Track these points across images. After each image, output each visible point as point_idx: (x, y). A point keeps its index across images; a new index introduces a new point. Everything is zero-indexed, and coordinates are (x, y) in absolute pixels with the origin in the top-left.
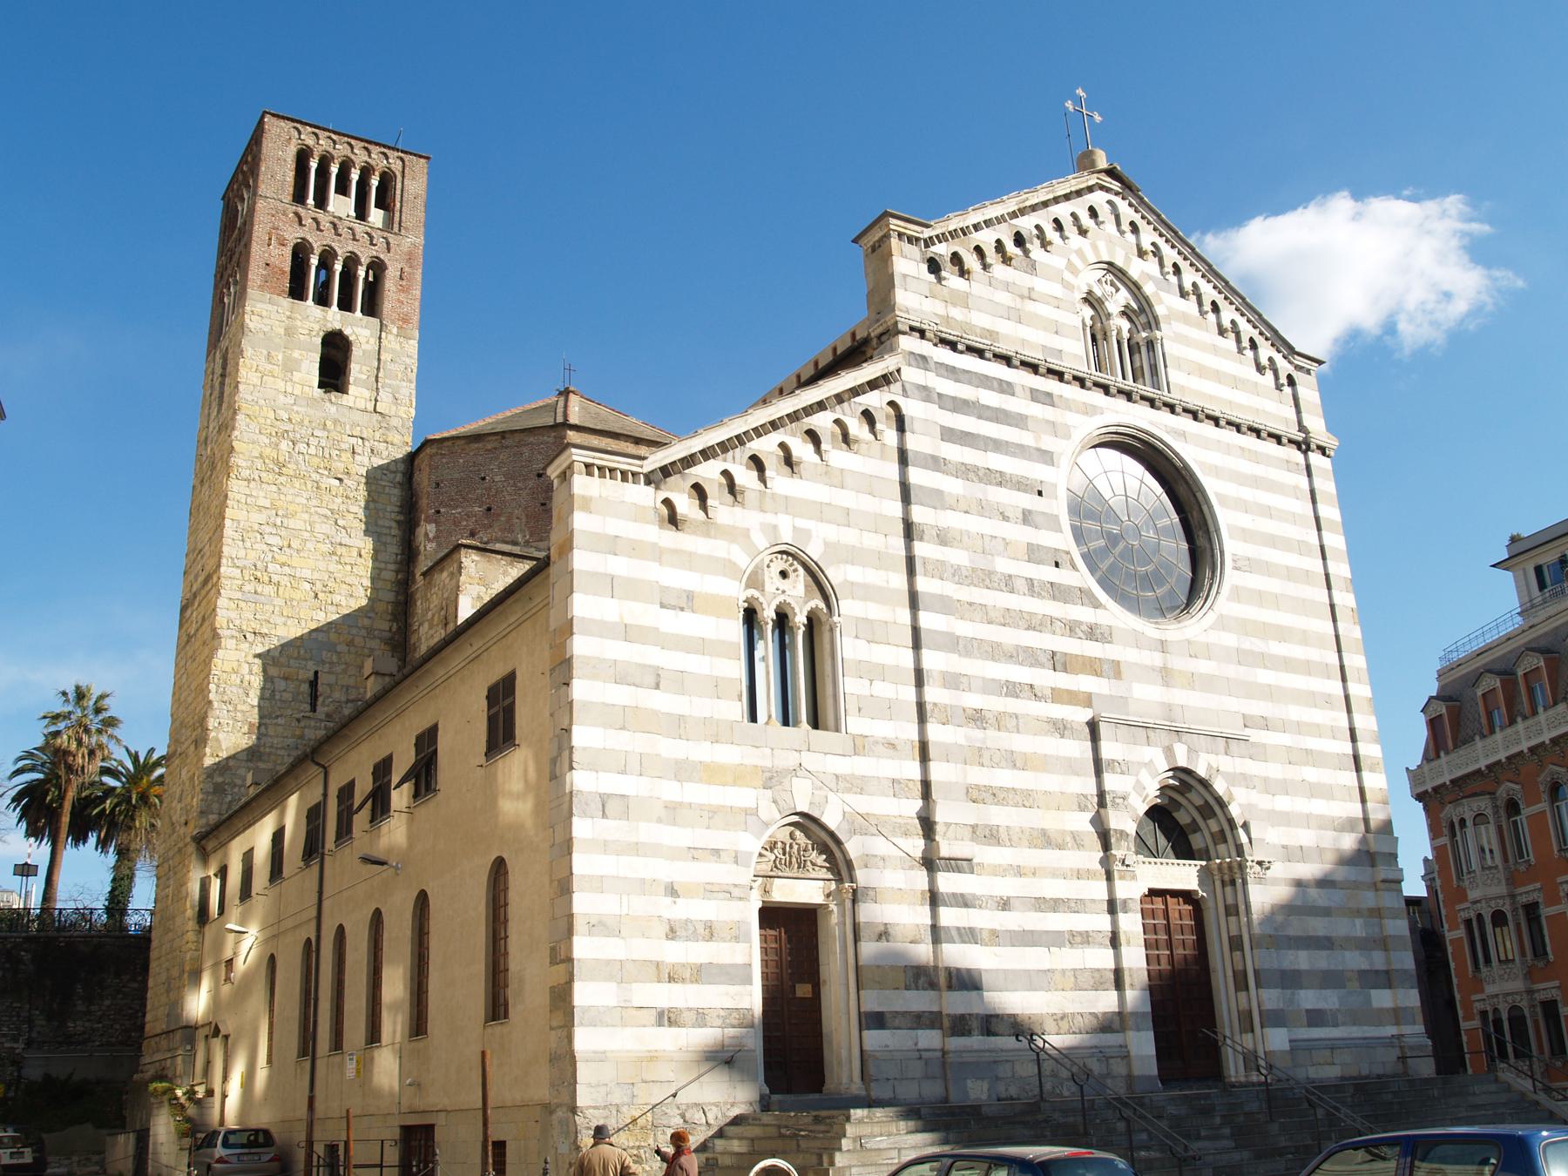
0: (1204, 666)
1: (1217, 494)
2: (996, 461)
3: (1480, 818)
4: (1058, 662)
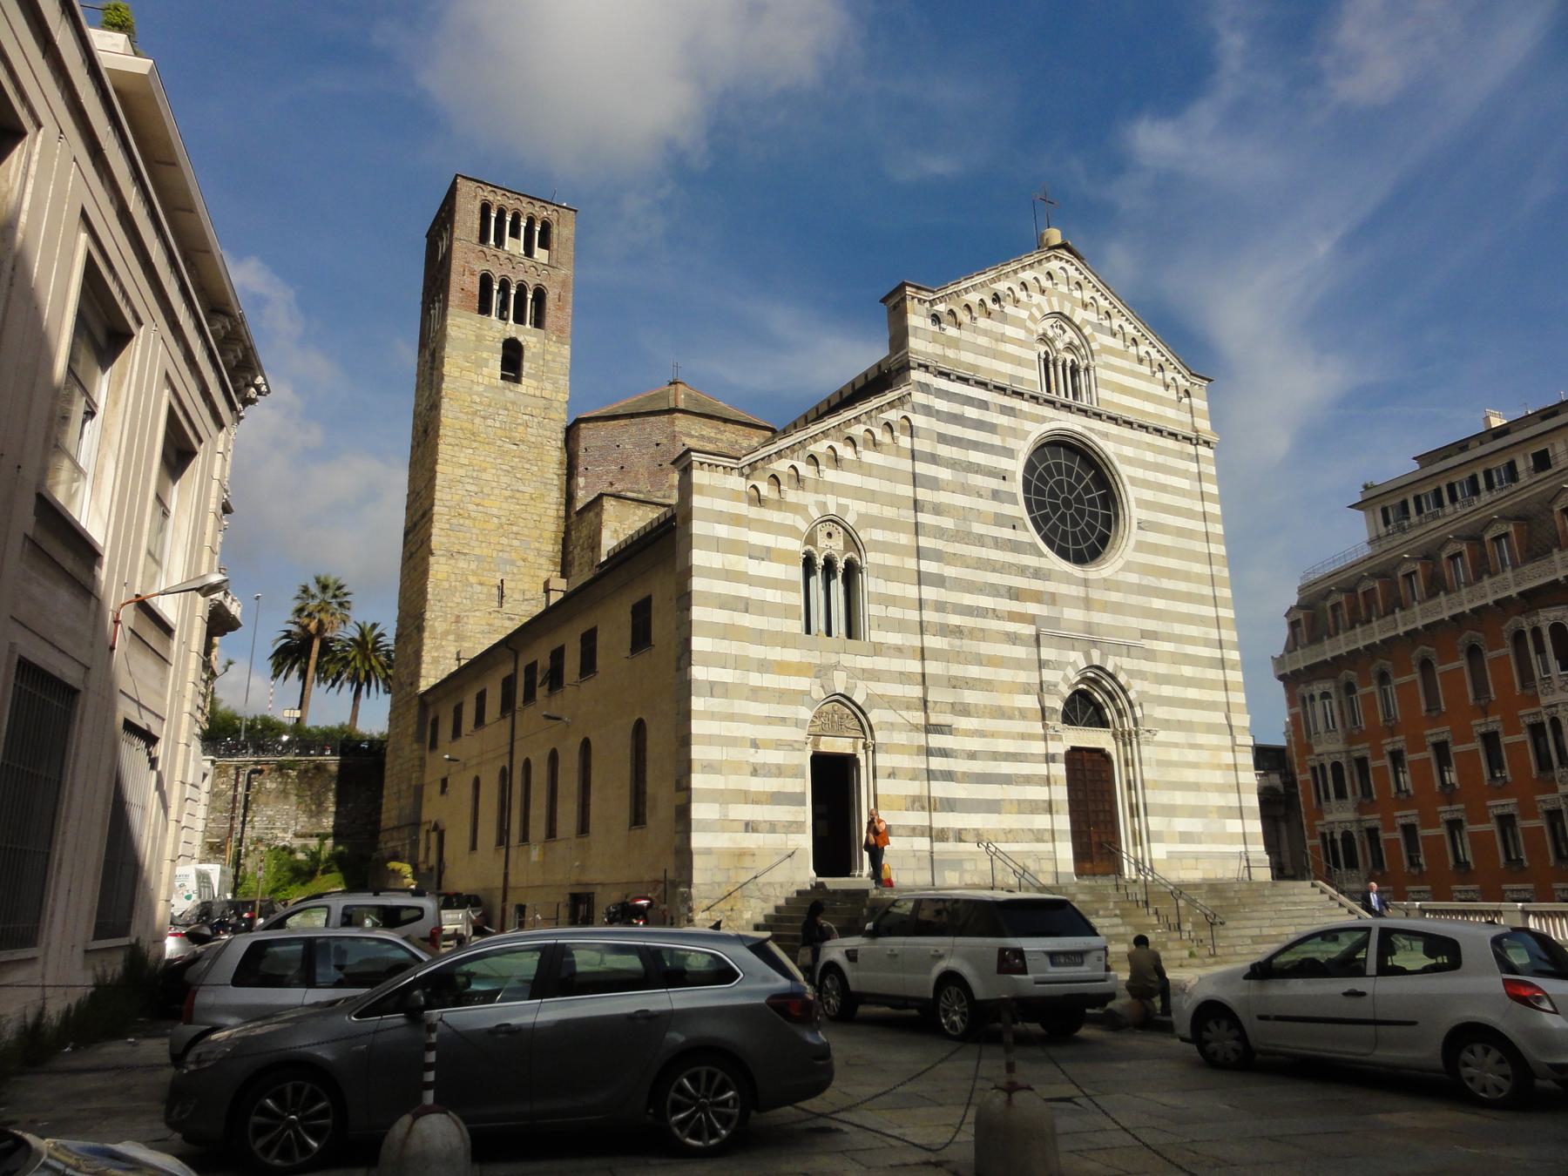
0: (1115, 596)
1: (1129, 477)
3: (1325, 695)
4: (1015, 594)
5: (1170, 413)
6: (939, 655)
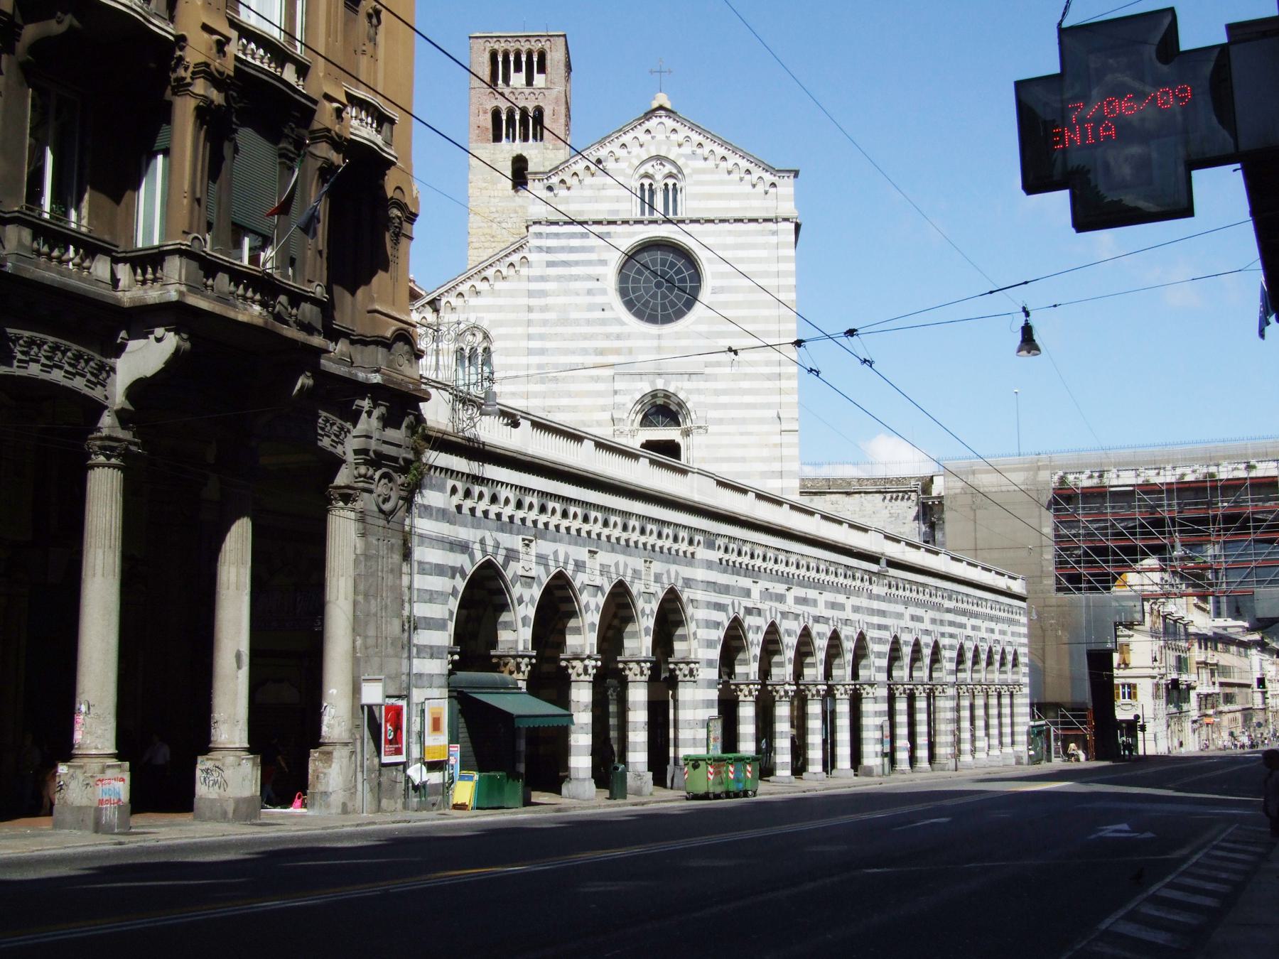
2: (575, 271)
5: (756, 203)
6: (536, 395)
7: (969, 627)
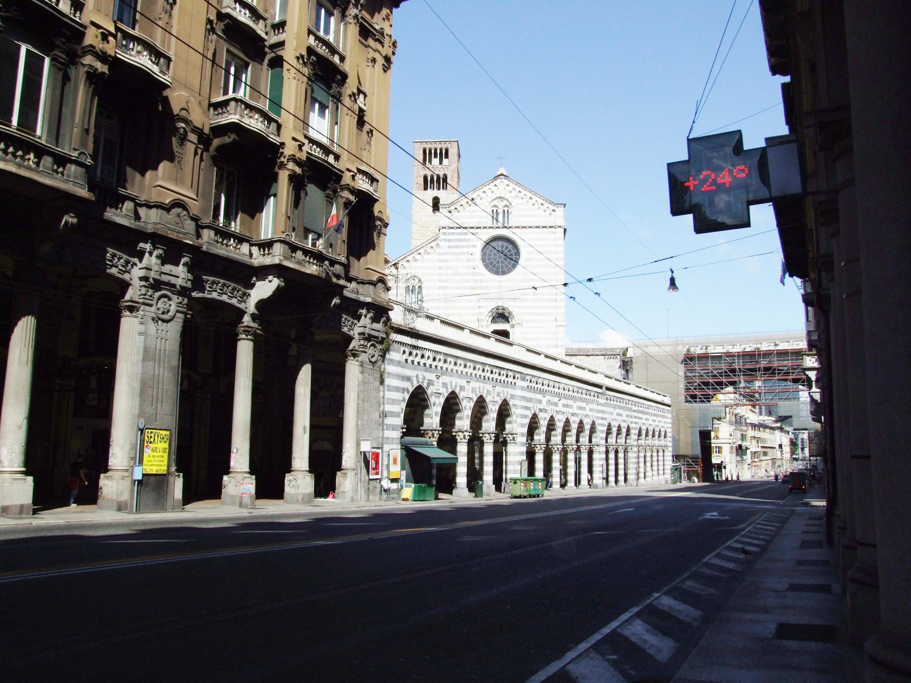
2: (461, 250)
7: (644, 419)
